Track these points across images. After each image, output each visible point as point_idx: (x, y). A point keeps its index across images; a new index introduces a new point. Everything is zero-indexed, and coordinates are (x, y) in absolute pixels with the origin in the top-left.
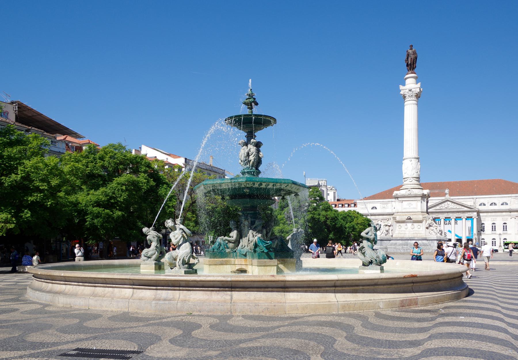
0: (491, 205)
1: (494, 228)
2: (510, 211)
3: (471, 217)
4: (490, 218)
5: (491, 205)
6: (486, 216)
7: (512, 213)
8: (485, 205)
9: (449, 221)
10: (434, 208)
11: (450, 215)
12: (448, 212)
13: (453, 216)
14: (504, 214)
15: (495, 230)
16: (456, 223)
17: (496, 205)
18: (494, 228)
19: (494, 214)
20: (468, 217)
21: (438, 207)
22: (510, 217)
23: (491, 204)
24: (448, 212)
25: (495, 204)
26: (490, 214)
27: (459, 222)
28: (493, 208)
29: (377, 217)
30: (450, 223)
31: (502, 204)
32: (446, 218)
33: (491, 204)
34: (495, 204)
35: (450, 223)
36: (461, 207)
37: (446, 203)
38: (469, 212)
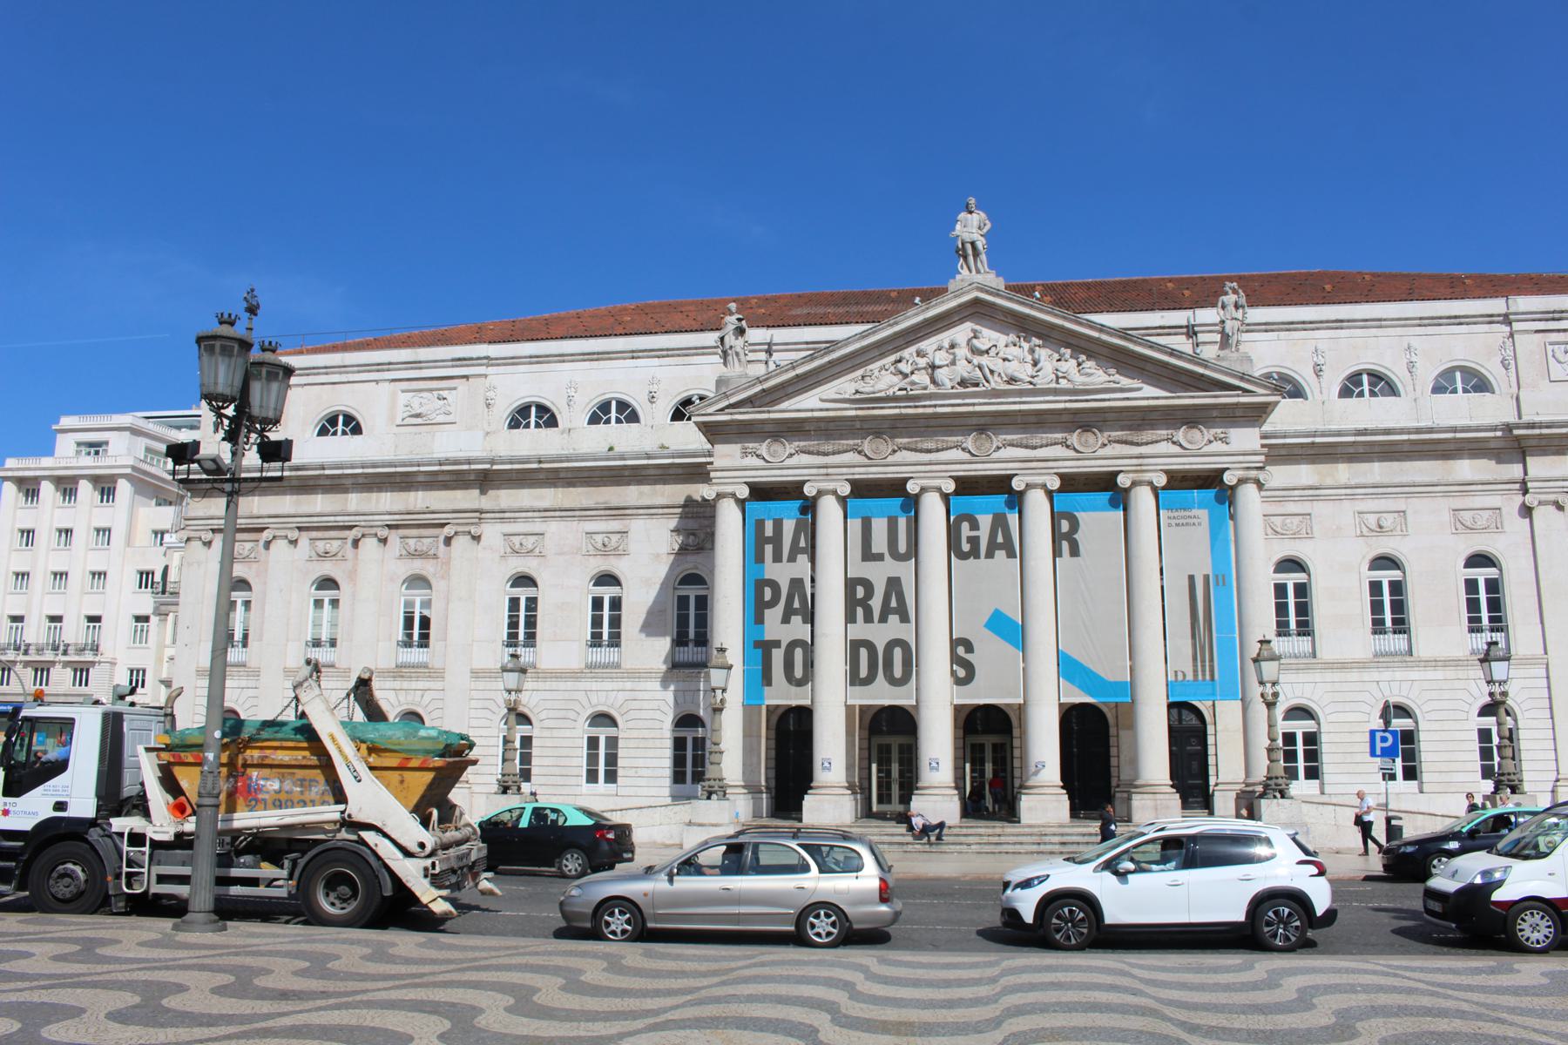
0: (1346, 392)
1: (1391, 609)
2: (1515, 445)
3: (1210, 480)
4: (1344, 514)
5: (1346, 392)
6: (1313, 492)
7: (1539, 466)
8: (1297, 392)
9: (999, 522)
10: (844, 386)
11: (1002, 456)
12: (985, 425)
13: (1034, 464)
14: (1465, 469)
15: (1401, 625)
16: (1065, 539)
17: (1392, 390)
18: (1391, 609)
19: (1376, 471)
20: (1181, 481)
21: (882, 379)
22: (1519, 499)
23: (1351, 386)
24: (985, 425)
25: (1382, 384)
26: (1343, 472)
27: (1096, 521)
28: (1371, 413)
29: (354, 501)
30: (1006, 544)
31: (1438, 389)
32: (967, 486)
33: (1351, 386)
34: (1382, 384)
35: (1006, 544)
36: (1097, 375)
37: (961, 333)
38: (1192, 418)
